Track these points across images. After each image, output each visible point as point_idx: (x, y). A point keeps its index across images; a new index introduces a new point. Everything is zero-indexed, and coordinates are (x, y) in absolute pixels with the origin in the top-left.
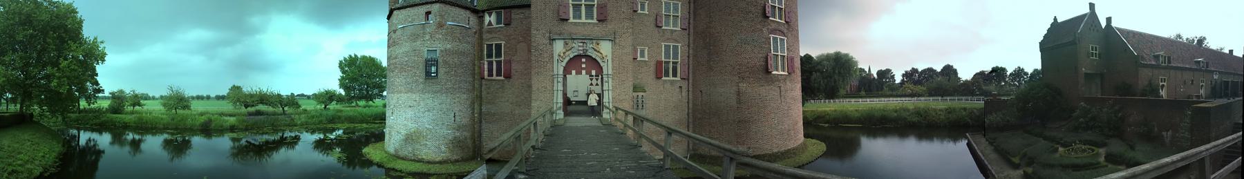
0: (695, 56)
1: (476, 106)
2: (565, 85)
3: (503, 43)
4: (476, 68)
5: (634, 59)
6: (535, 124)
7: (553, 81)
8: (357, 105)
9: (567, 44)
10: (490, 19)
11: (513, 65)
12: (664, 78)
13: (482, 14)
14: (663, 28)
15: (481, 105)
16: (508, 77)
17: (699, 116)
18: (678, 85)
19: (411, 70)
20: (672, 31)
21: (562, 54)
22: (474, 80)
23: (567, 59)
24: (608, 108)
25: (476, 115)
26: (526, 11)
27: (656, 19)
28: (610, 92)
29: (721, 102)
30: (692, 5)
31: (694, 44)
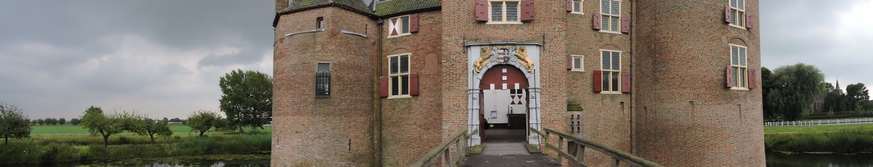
0: (638, 65)
1: (376, 131)
2: (481, 103)
3: (410, 54)
4: (375, 86)
5: (568, 69)
6: (447, 151)
7: (467, 97)
9: (484, 51)
10: (394, 27)
11: (420, 80)
12: (603, 92)
13: (381, 21)
14: (601, 31)
15: (380, 130)
16: (415, 95)
17: (644, 138)
18: (619, 100)
20: (611, 36)
21: (478, 64)
22: (373, 100)
23: (484, 70)
24: (535, 131)
25: (376, 142)
26: (436, 15)
27: (593, 21)
28: (539, 111)
31: (637, 51)
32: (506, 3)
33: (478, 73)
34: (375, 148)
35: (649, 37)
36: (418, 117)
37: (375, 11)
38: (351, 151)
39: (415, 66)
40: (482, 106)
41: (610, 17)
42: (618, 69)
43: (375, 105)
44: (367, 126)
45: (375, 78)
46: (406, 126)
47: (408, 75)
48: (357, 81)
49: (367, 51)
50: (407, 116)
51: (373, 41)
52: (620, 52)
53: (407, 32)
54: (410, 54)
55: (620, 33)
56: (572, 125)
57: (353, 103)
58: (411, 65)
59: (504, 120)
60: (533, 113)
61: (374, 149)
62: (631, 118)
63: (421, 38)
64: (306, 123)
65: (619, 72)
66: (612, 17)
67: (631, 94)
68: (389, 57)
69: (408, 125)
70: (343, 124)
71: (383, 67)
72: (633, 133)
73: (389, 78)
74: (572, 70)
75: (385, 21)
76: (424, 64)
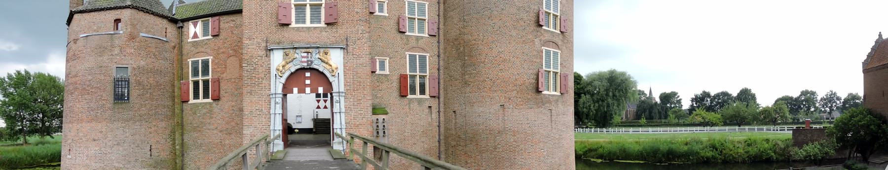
1: (177, 136)
2: (284, 107)
3: (210, 58)
5: (372, 72)
8: (26, 142)
9: (287, 55)
10: (194, 30)
11: (221, 84)
12: (409, 96)
14: (407, 33)
15: (182, 135)
16: (217, 99)
17: (453, 143)
18: (428, 104)
19: (95, 93)
20: (418, 39)
21: (281, 68)
24: (340, 136)
25: (177, 147)
27: (398, 23)
28: (343, 115)
29: (479, 124)
30: (442, 5)
31: (445, 53)
32: (310, 5)
33: (281, 77)
34: (177, 154)
35: (457, 39)
36: (219, 122)
37: (175, 14)
38: (152, 157)
39: (215, 70)
40: (284, 111)
41: (416, 19)
42: (426, 72)
43: (176, 110)
44: (168, 132)
45: (176, 82)
46: (208, 131)
47: (209, 79)
48: (158, 86)
49: (167, 55)
50: (208, 121)
51: (173, 44)
52: (428, 55)
53: (208, 35)
54: (210, 58)
55: (427, 36)
56: (377, 129)
57: (153, 108)
58: (212, 69)
59: (310, 125)
60: (337, 117)
61: (176, 154)
62: (439, 122)
63: (222, 41)
64: (104, 130)
65: (426, 76)
66: (418, 19)
67: (439, 98)
68: (190, 61)
69: (209, 129)
70: (143, 130)
71: (184, 71)
72: (441, 138)
73: (190, 82)
74: (376, 73)
75: (185, 24)
76: (226, 68)
